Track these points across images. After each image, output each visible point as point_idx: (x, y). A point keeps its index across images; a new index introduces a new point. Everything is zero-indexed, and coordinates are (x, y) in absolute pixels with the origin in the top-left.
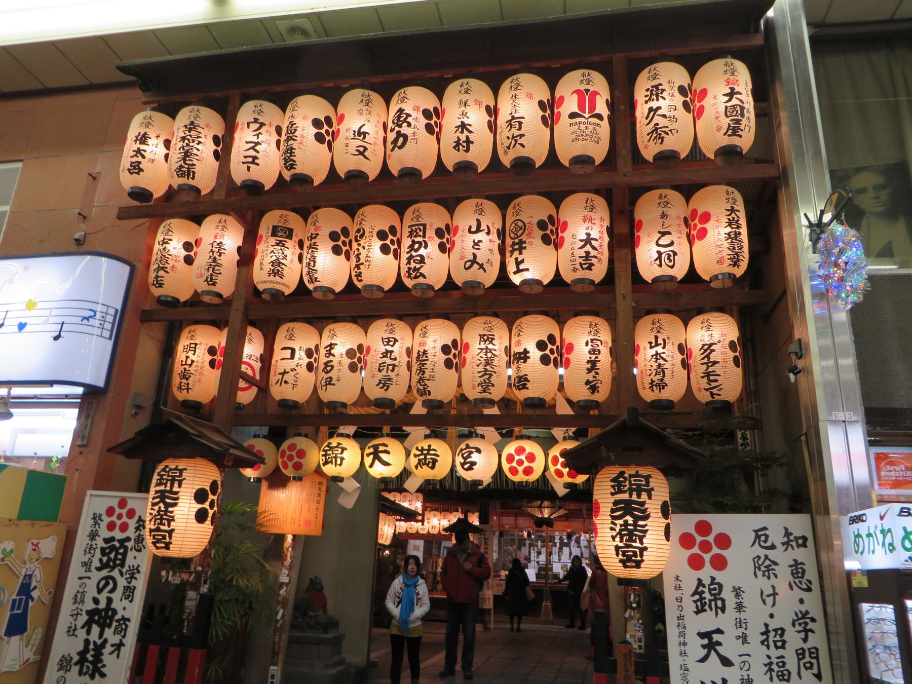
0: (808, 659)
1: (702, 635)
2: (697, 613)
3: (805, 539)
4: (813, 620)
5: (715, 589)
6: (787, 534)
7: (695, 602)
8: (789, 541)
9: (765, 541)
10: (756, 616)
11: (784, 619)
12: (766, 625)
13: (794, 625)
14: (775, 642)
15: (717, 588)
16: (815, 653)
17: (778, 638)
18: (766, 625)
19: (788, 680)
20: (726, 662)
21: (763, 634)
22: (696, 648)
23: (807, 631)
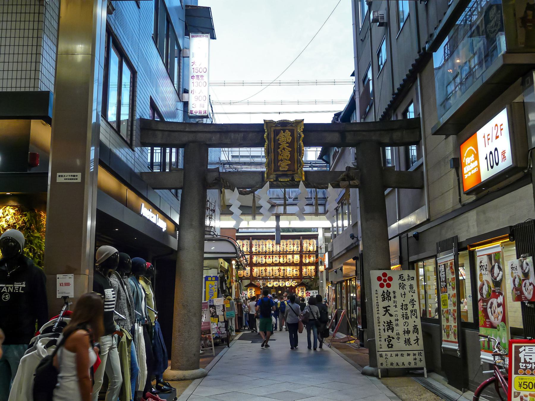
1: (384, 308)
3: (413, 278)
6: (409, 276)
10: (400, 300)
11: (407, 302)
15: (388, 293)
22: (382, 311)
23: (413, 305)
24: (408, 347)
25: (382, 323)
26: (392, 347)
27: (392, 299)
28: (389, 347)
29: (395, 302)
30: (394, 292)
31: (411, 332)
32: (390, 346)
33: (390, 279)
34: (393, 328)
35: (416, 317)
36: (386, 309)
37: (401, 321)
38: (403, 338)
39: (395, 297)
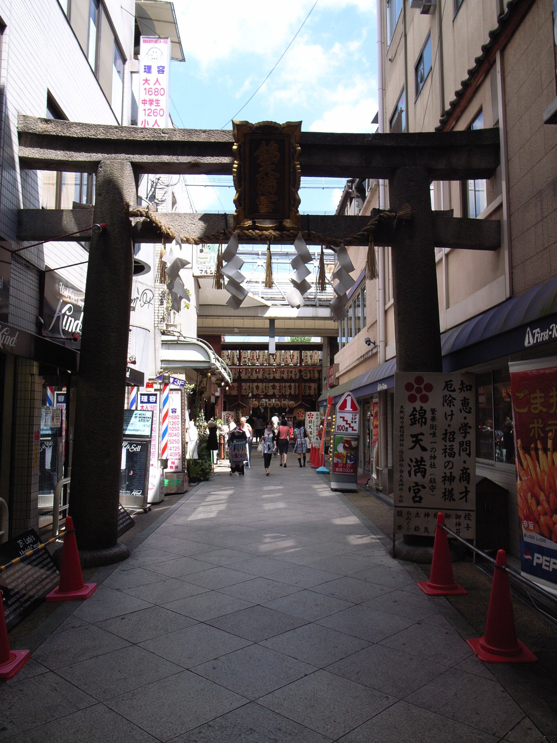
0: (465, 446)
1: (412, 436)
2: (411, 425)
3: (471, 386)
4: (470, 427)
5: (422, 413)
6: (462, 383)
7: (411, 419)
8: (463, 387)
9: (450, 388)
12: (446, 430)
13: (460, 430)
14: (449, 439)
15: (423, 412)
16: (469, 443)
17: (451, 436)
18: (446, 430)
19: (454, 457)
20: (424, 449)
21: (443, 435)
23: (466, 433)
24: (448, 504)
25: (407, 461)
26: (420, 501)
27: (429, 422)
28: (415, 502)
29: (432, 427)
30: (433, 411)
31: (457, 479)
32: (417, 499)
33: (429, 388)
34: (425, 470)
35: (469, 455)
36: (417, 439)
37: (441, 460)
38: (441, 487)
39: (433, 419)
